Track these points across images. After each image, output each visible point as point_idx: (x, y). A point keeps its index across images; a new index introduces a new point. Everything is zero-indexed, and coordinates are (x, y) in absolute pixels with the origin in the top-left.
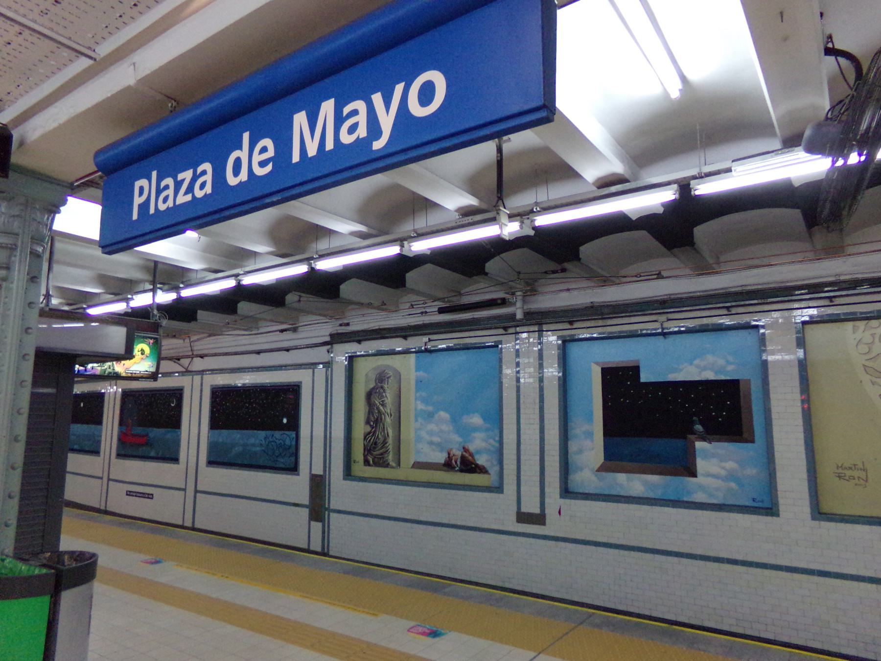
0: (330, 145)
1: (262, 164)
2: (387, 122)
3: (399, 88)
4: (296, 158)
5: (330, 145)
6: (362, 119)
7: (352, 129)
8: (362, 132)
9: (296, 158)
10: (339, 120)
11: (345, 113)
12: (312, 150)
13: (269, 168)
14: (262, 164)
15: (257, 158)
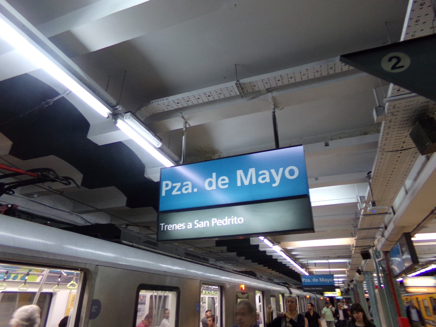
0: (254, 182)
1: (223, 185)
2: (278, 179)
3: (281, 170)
4: (239, 184)
5: (254, 182)
6: (267, 176)
7: (264, 179)
8: (268, 180)
9: (239, 184)
10: (257, 176)
11: (260, 174)
12: (246, 183)
13: (227, 186)
14: (223, 185)
15: (220, 182)
